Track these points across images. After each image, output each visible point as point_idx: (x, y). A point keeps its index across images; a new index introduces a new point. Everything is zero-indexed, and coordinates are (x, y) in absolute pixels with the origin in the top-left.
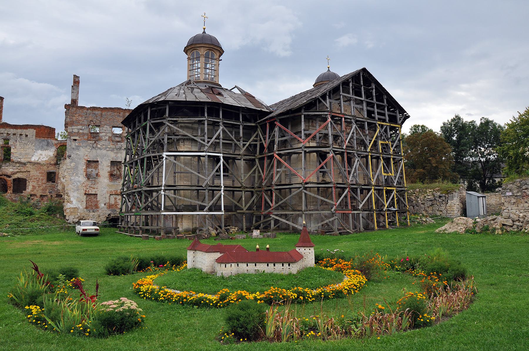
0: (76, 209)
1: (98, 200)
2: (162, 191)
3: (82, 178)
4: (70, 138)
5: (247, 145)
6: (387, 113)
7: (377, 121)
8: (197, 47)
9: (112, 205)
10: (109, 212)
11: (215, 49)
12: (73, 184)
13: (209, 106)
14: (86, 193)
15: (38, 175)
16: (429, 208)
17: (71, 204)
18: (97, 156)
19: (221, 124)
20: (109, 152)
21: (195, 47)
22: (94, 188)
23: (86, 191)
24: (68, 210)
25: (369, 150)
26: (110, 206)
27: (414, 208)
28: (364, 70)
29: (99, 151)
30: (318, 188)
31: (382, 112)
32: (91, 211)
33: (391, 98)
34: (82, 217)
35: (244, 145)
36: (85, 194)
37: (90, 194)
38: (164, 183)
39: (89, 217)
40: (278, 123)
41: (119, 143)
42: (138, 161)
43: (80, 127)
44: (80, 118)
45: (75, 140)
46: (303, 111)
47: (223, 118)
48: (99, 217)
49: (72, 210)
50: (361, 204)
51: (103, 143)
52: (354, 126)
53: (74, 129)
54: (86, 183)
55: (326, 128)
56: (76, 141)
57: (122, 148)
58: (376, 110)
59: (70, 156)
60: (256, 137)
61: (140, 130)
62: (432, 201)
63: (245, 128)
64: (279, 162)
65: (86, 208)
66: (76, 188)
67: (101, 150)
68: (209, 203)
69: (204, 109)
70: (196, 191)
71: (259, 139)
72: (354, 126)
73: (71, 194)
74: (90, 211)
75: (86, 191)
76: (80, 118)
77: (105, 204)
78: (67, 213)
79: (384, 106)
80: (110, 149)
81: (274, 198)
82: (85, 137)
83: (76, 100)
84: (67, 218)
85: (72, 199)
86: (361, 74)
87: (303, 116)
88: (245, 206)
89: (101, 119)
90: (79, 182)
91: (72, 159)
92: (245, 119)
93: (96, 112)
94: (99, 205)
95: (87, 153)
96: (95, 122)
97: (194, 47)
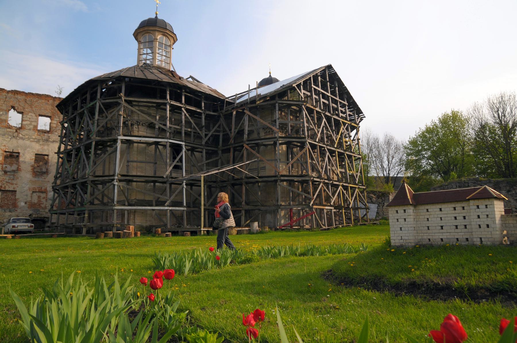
1: (17, 197)
2: (115, 180)
5: (209, 135)
8: (150, 30)
9: (35, 204)
10: (31, 212)
13: (171, 89)
20: (34, 144)
21: (148, 30)
22: (12, 184)
26: (32, 205)
29: (21, 142)
37: (7, 191)
38: (117, 171)
40: (247, 112)
41: (46, 134)
42: (81, 147)
46: (277, 98)
57: (50, 140)
60: (219, 127)
61: (85, 112)
63: (207, 117)
67: (24, 140)
71: (222, 129)
74: (5, 211)
77: (26, 203)
80: (35, 140)
93: (19, 97)
94: (19, 204)
95: (5, 142)
97: (147, 30)
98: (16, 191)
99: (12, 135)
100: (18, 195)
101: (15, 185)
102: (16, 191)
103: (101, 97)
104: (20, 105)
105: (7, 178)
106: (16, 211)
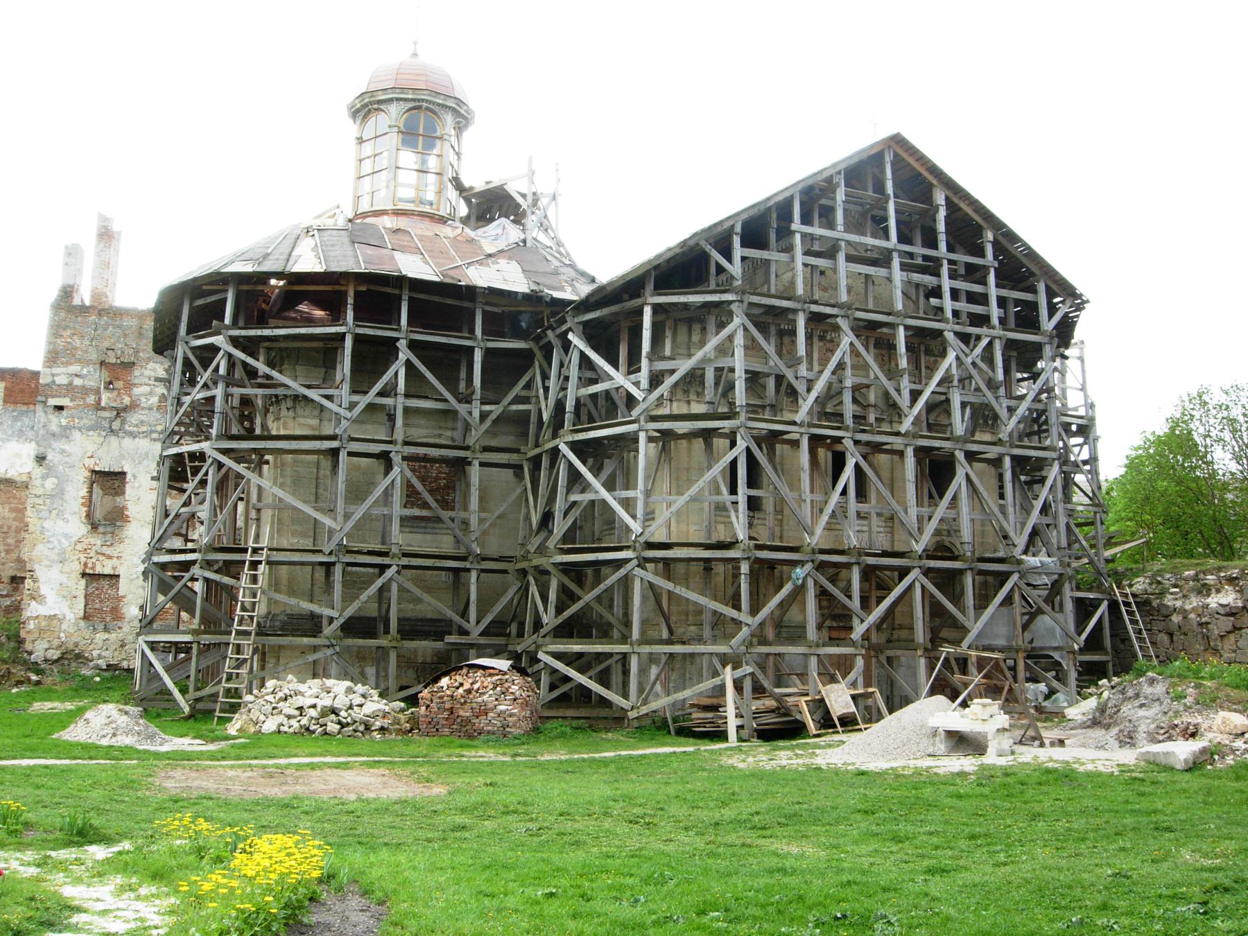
0: (55, 622)
1: (121, 593)
3: (77, 527)
4: (44, 403)
6: (993, 292)
7: (946, 321)
11: (439, 105)
12: (49, 542)
13: (363, 288)
14: (88, 571)
15: (7, 514)
16: (1226, 641)
17: (40, 604)
18: (122, 456)
19: (402, 344)
22: (110, 557)
23: (86, 565)
24: (32, 622)
25: (906, 425)
27: (1172, 641)
28: (898, 141)
29: (128, 442)
30: (707, 561)
31: (977, 288)
32: (101, 626)
33: (1012, 237)
34: (71, 647)
35: (484, 416)
36: (84, 575)
37: (99, 575)
39: (91, 647)
43: (75, 368)
44: (77, 342)
45: (60, 408)
47: (409, 323)
48: (122, 646)
49: (43, 624)
50: (862, 621)
51: (144, 418)
52: (847, 339)
53: (58, 375)
54: (87, 541)
55: (725, 349)
56: (64, 413)
58: (947, 284)
59: (44, 458)
60: (528, 386)
62: (1233, 614)
64: (575, 476)
65: (86, 617)
66: (58, 554)
67: (134, 437)
68: (343, 610)
69: (344, 295)
70: (324, 568)
72: (847, 339)
73: (40, 572)
74: (95, 629)
75: (86, 565)
76: (77, 342)
78: (28, 632)
79: (985, 269)
81: (552, 596)
82: (88, 400)
83: (72, 287)
84: (28, 646)
85: (44, 590)
86: (888, 159)
87: (648, 311)
88: (478, 622)
89: (137, 344)
90: (66, 536)
91: (49, 468)
92: (495, 326)
96: (119, 352)
98: (118, 576)
99: (107, 425)
100: (124, 587)
101: (115, 560)
102: (118, 576)
103: (188, 334)
104: (126, 345)
105: (99, 542)
106: (120, 628)
